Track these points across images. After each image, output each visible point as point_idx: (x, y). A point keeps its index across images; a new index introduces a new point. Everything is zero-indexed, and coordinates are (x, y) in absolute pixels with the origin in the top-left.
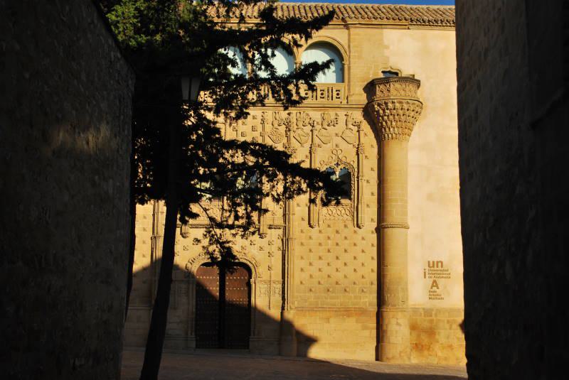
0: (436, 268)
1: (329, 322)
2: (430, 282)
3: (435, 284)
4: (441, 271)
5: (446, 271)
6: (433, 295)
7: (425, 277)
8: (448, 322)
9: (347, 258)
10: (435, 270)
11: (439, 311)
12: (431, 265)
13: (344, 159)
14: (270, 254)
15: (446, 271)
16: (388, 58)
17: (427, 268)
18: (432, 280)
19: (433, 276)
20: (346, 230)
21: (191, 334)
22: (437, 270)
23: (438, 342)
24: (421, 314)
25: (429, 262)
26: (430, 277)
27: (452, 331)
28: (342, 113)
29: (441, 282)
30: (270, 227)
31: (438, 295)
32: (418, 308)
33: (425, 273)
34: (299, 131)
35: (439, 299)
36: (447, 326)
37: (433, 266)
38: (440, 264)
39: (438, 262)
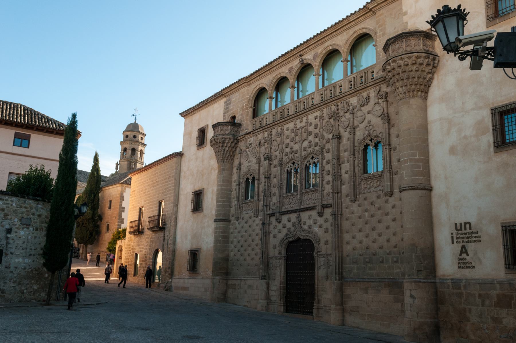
0: (463, 231)
1: (367, 293)
2: (458, 247)
3: (464, 250)
4: (469, 233)
5: (475, 233)
6: (463, 264)
7: (453, 243)
8: (480, 296)
9: (381, 227)
10: (465, 234)
11: (468, 283)
12: (459, 228)
13: (375, 134)
14: (326, 231)
15: (475, 233)
16: (407, 23)
17: (455, 232)
18: (461, 245)
19: (461, 240)
20: (379, 200)
21: (281, 301)
22: (465, 234)
23: (469, 321)
24: (449, 285)
25: (456, 224)
26: (458, 242)
27: (486, 308)
28: (372, 93)
29: (471, 247)
30: (324, 207)
31: (469, 263)
32: (447, 279)
33: (452, 237)
34: (343, 119)
35: (469, 268)
36: (478, 301)
37: (461, 229)
38: (468, 226)
39: (465, 224)
